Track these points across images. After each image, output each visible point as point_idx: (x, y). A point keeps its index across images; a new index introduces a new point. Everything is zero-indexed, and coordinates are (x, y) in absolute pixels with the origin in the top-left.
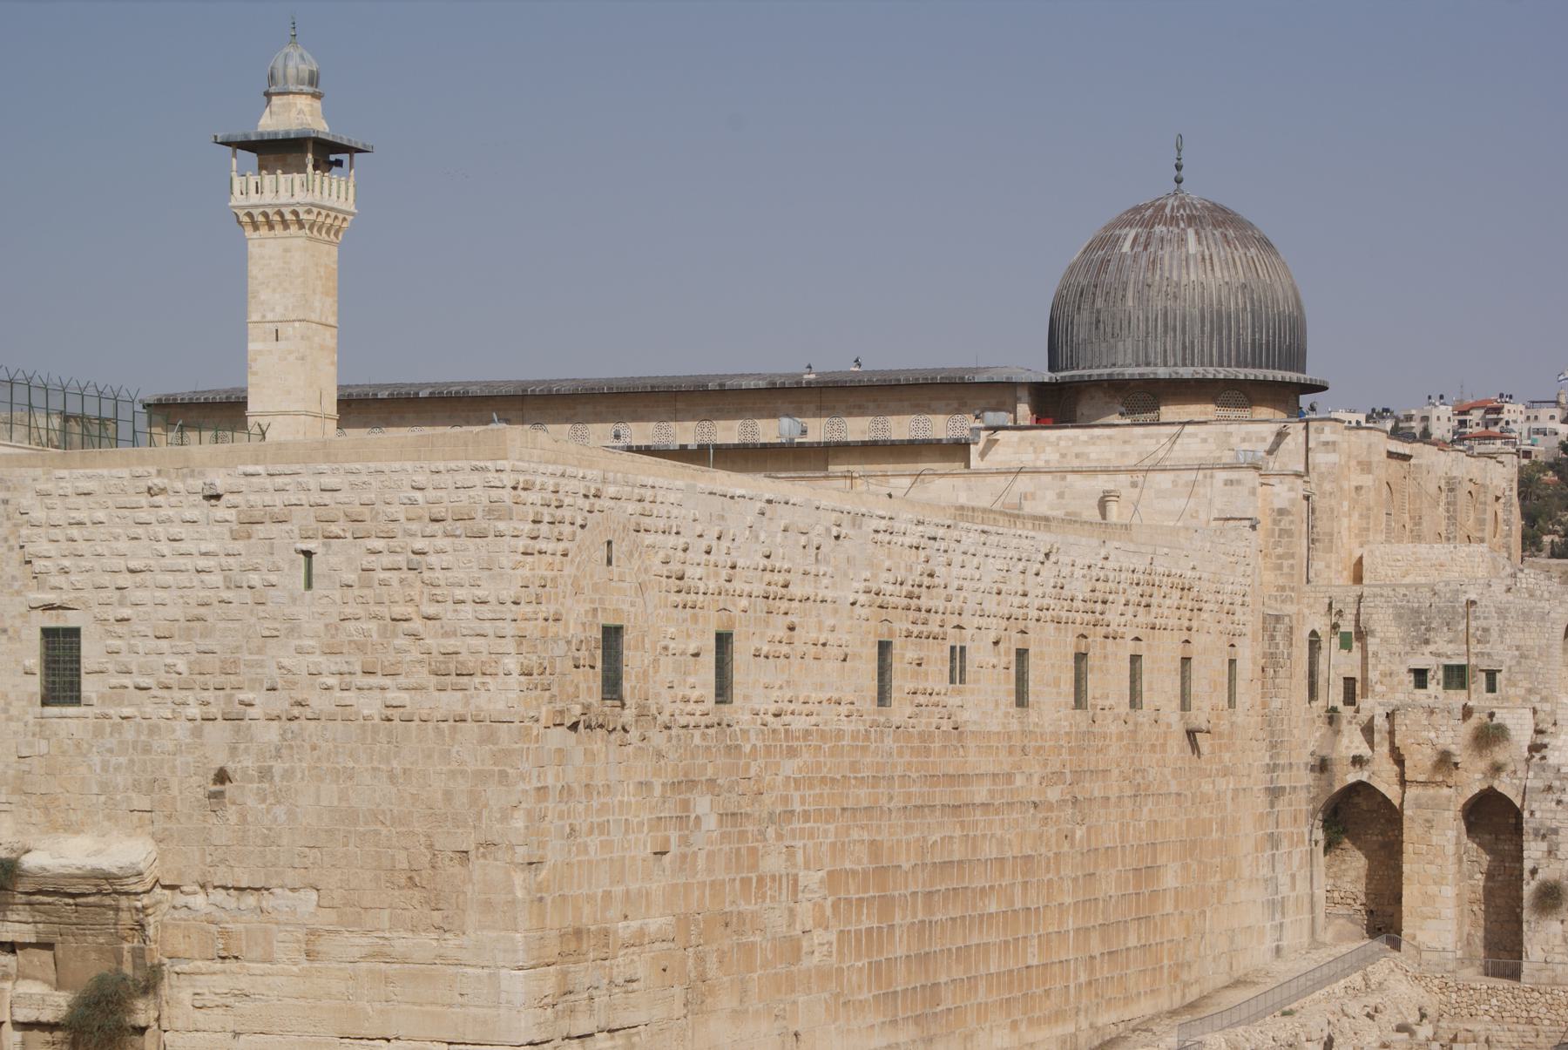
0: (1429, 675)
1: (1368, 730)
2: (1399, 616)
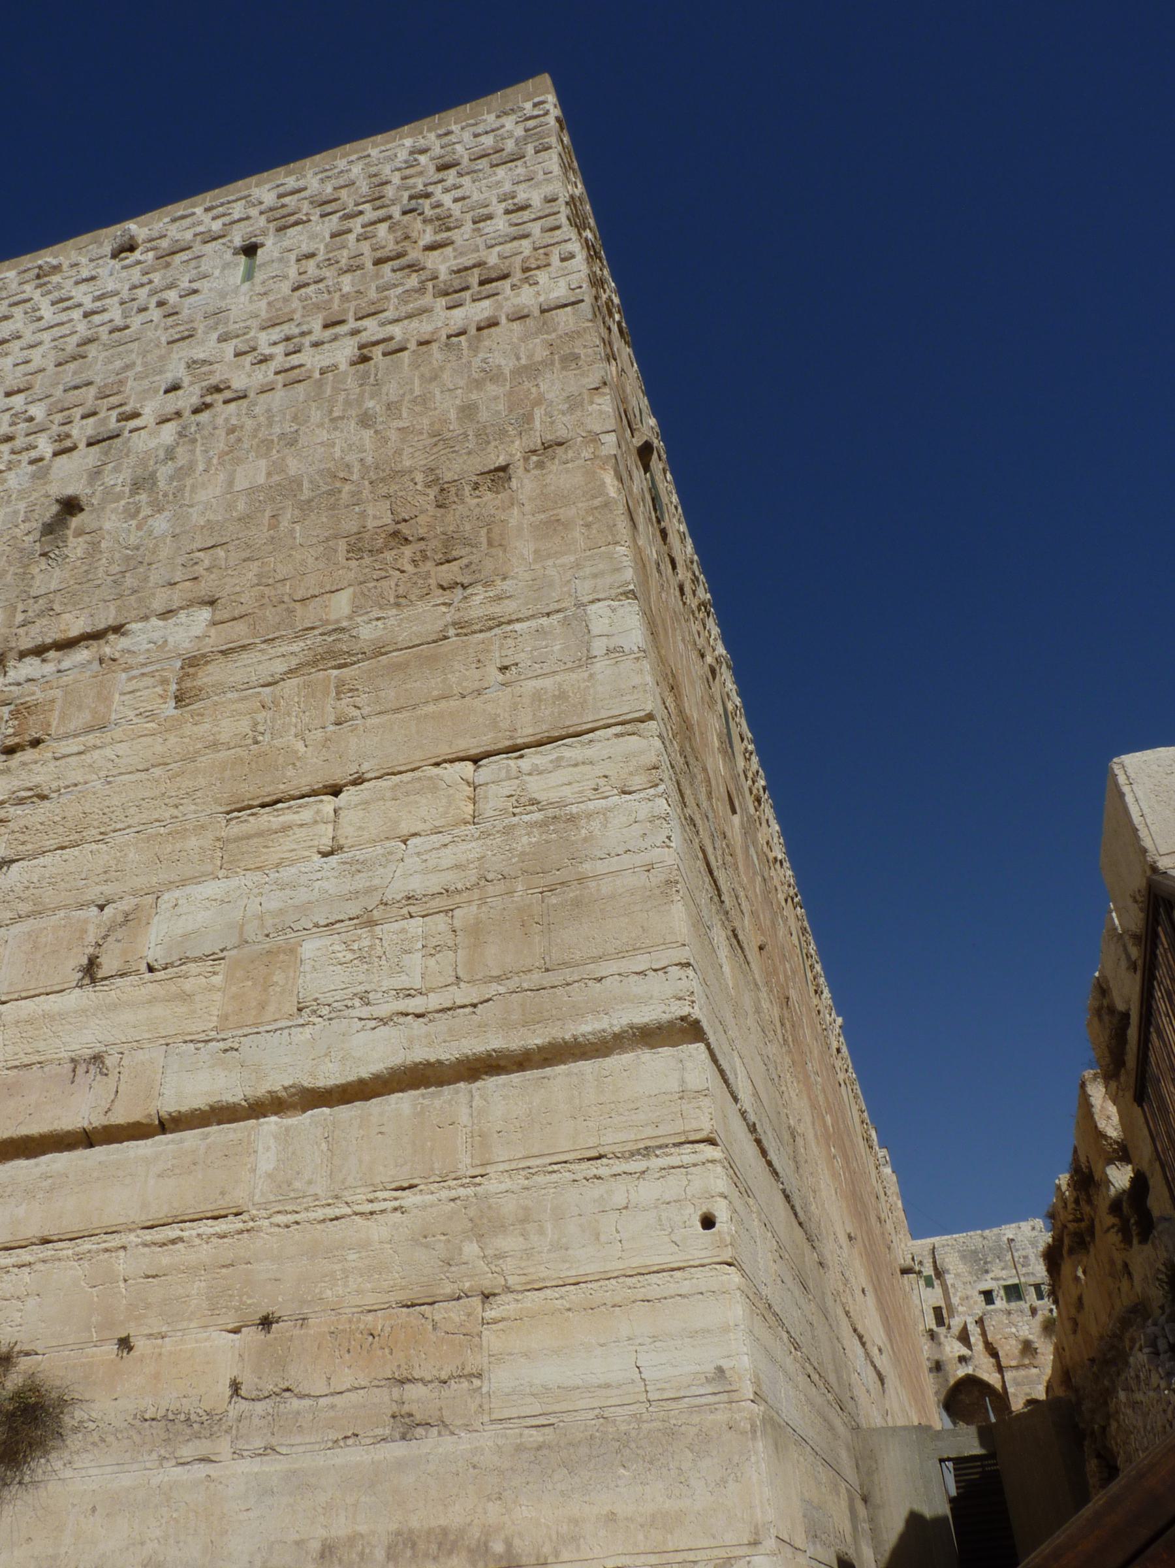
0: (994, 1294)
1: (964, 1337)
2: (963, 1257)
